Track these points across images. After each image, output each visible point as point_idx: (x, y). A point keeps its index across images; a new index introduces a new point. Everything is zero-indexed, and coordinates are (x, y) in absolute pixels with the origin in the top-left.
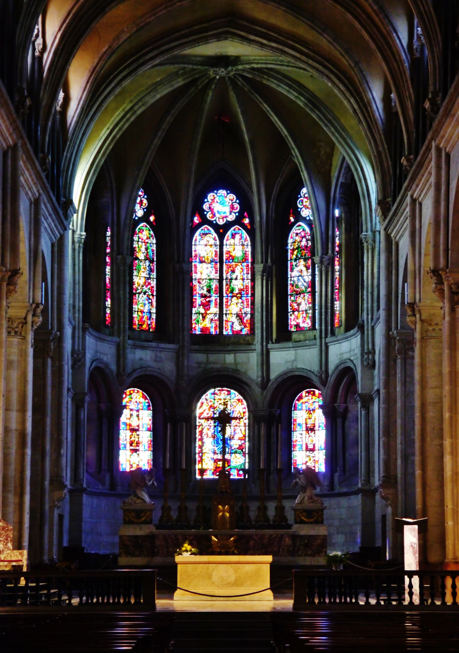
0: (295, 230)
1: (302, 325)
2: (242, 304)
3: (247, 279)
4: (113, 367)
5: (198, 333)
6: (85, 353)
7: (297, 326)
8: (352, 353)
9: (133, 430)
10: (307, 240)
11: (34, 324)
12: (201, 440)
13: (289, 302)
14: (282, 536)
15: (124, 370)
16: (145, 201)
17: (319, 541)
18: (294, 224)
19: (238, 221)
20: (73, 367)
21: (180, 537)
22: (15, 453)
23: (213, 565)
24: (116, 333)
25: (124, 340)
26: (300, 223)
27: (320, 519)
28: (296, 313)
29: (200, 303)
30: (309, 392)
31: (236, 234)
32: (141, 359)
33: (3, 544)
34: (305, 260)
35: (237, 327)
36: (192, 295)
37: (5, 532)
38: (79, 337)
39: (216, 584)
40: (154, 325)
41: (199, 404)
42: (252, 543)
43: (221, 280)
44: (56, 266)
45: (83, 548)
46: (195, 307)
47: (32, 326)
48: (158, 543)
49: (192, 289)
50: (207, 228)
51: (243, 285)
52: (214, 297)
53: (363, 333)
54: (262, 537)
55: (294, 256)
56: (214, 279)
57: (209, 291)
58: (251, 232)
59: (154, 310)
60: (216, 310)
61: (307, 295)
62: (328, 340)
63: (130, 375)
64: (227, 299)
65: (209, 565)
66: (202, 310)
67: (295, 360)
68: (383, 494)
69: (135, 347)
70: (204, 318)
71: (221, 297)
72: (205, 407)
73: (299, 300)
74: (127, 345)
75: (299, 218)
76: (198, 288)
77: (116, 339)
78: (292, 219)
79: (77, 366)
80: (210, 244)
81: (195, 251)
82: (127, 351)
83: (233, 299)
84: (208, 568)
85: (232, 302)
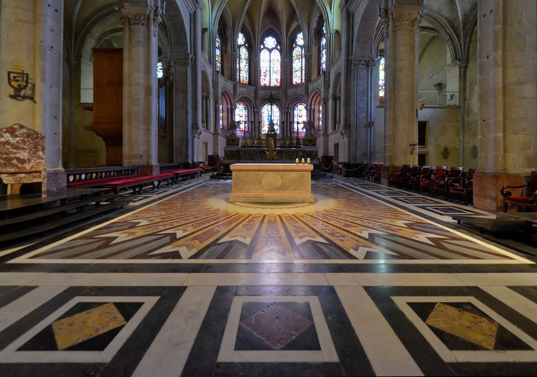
0: (295, 50)
1: (297, 82)
4: (232, 93)
5: (263, 85)
6: (218, 82)
7: (296, 82)
8: (318, 86)
9: (241, 116)
10: (300, 52)
11: (155, 21)
12: (264, 120)
13: (293, 74)
14: (298, 151)
15: (236, 94)
16: (244, 39)
17: (314, 154)
18: (295, 47)
19: (276, 48)
20: (213, 87)
21: (251, 151)
22: (144, 98)
23: (263, 172)
24: (233, 80)
25: (236, 83)
26: (297, 47)
27: (315, 144)
28: (295, 78)
30: (300, 104)
32: (242, 91)
33: (29, 153)
34: (299, 59)
35: (276, 83)
36: (260, 73)
37: (32, 139)
38: (215, 75)
39: (265, 188)
40: (248, 82)
41: (263, 109)
42: (284, 154)
43: (270, 67)
44: (192, 25)
45: (218, 156)
47: (154, 22)
48: (241, 154)
49: (260, 71)
52: (268, 73)
53: (325, 75)
54: (289, 151)
55: (295, 59)
57: (266, 71)
58: (281, 51)
59: (248, 77)
60: (269, 78)
61: (300, 72)
62: (308, 83)
63: (238, 96)
65: (259, 172)
66: (264, 78)
67: (296, 92)
68: (344, 132)
69: (241, 86)
70: (264, 80)
71: (270, 73)
72: (265, 109)
73: (297, 73)
74: (237, 85)
75: (297, 45)
77: (233, 82)
78: (294, 46)
79: (215, 87)
82: (237, 87)
84: (258, 175)
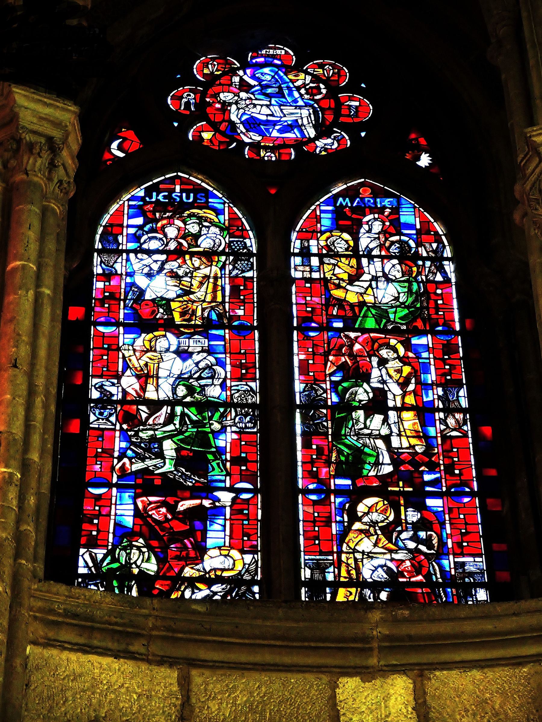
2: (422, 534)
3: (449, 411)
29: (128, 522)
31: (362, 210)
46: (92, 543)
50: (183, 181)
51: (426, 437)
56: (228, 404)
64: (326, 502)
76: (119, 444)
80: (205, 244)
81: (107, 276)
83: (361, 508)
85: (354, 517)
